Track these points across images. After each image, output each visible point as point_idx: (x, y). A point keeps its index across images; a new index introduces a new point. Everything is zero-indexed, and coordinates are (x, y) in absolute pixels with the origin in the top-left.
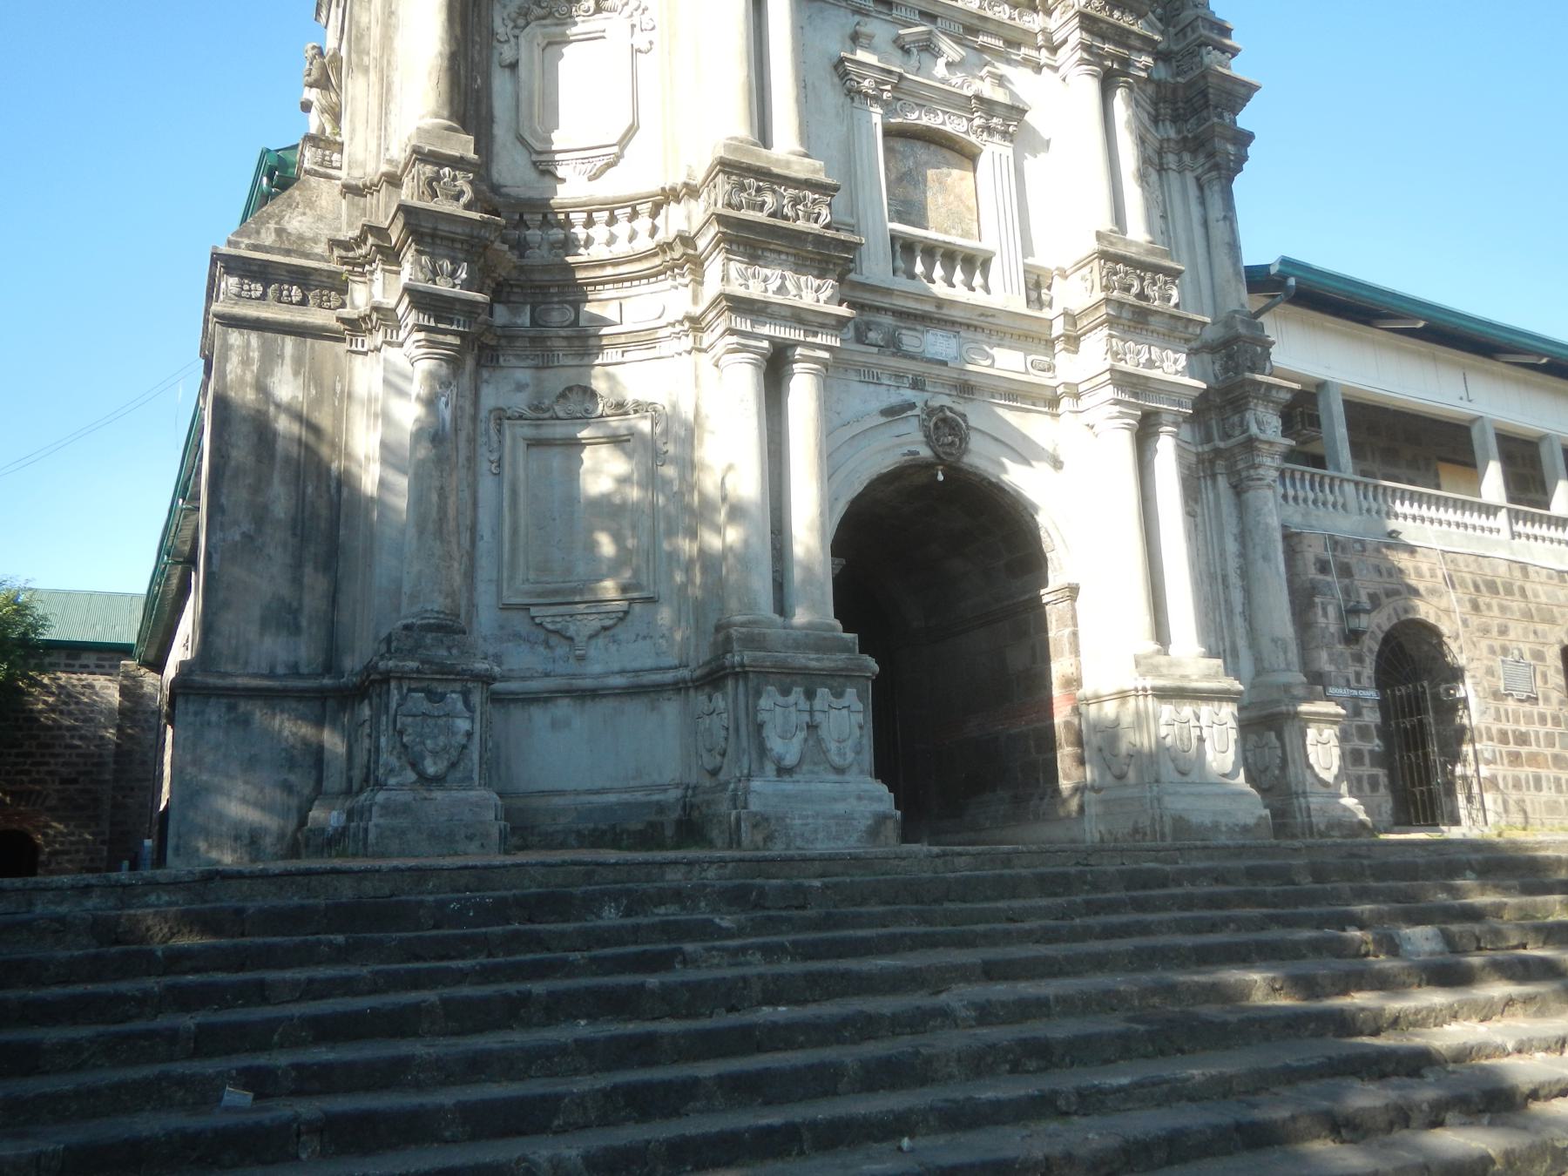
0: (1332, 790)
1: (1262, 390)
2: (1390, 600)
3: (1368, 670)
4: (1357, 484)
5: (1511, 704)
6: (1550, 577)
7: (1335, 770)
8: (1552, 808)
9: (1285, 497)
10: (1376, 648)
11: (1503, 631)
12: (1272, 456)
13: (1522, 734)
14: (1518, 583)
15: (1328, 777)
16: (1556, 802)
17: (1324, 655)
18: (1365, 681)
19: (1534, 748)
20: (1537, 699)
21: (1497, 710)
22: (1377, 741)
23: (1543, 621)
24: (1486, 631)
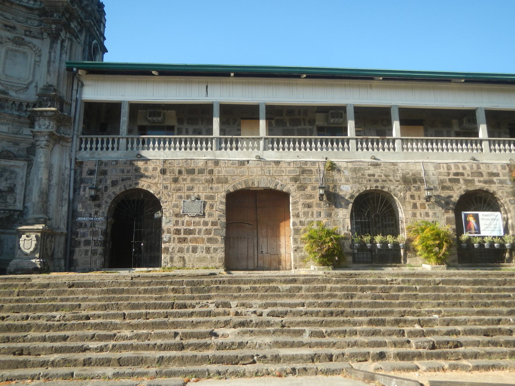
0: (30, 257)
1: (39, 113)
2: (124, 182)
3: (104, 209)
4: (127, 139)
5: (187, 218)
6: (233, 164)
7: (32, 249)
8: (201, 260)
9: (86, 149)
10: (110, 201)
11: (190, 189)
12: (44, 136)
13: (190, 230)
14: (210, 168)
15: (28, 252)
16: (204, 257)
17: (80, 206)
18: (100, 213)
19: (197, 236)
20: (204, 215)
21: (177, 223)
22: (100, 236)
23: (218, 183)
24: (179, 190)
